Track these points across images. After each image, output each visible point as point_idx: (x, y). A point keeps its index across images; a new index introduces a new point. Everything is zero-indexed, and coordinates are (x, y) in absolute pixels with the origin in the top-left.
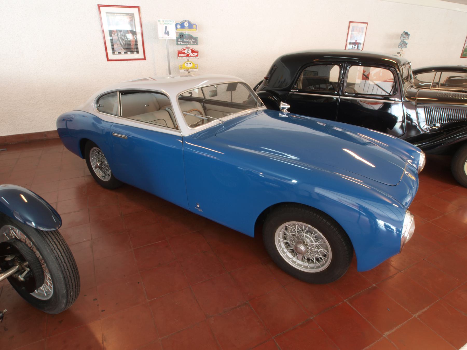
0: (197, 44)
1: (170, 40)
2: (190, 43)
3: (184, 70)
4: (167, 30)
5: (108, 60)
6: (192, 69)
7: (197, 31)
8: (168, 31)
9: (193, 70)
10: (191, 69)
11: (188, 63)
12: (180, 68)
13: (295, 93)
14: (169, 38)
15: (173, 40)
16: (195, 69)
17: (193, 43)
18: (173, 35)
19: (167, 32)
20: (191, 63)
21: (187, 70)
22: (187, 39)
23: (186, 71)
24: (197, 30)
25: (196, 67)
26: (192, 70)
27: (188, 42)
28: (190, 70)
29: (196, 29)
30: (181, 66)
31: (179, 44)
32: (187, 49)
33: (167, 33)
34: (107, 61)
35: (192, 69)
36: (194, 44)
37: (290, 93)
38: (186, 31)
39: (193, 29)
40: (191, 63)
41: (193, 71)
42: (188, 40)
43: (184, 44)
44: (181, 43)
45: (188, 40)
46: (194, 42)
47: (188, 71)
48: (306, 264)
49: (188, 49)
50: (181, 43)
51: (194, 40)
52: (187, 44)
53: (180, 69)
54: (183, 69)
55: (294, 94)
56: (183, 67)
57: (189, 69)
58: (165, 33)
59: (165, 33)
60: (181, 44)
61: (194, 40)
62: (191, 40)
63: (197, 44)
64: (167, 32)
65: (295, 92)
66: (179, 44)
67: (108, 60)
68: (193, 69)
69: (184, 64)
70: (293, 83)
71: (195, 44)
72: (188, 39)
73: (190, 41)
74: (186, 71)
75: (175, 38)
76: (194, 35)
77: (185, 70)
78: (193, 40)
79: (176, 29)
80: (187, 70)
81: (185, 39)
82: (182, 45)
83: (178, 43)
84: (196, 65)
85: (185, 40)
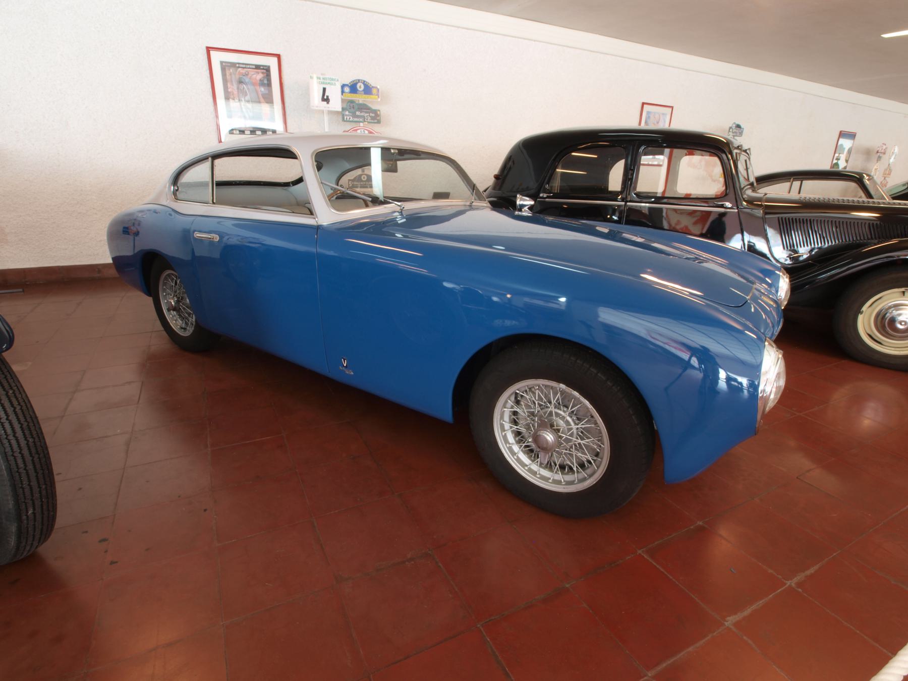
0: (379, 122)
1: (331, 113)
2: (367, 120)
4: (327, 94)
7: (379, 100)
8: (327, 97)
13: (547, 199)
14: (328, 108)
15: (337, 112)
17: (371, 120)
18: (336, 103)
19: (325, 97)
22: (361, 112)
24: (379, 97)
27: (364, 117)
29: (377, 97)
31: (347, 118)
32: (360, 130)
33: (325, 99)
36: (373, 121)
37: (538, 199)
38: (360, 98)
39: (372, 96)
42: (362, 114)
43: (356, 119)
44: (350, 118)
45: (362, 114)
46: (373, 118)
48: (559, 476)
49: (362, 130)
50: (350, 118)
51: (373, 115)
52: (361, 120)
55: (545, 201)
58: (323, 100)
59: (323, 100)
60: (351, 120)
61: (373, 115)
62: (368, 114)
63: (379, 122)
64: (325, 97)
65: (548, 197)
66: (347, 118)
70: (544, 182)
71: (376, 121)
72: (364, 112)
73: (367, 116)
75: (340, 110)
76: (374, 107)
78: (371, 114)
79: (342, 94)
81: (357, 113)
82: (351, 121)
83: (345, 117)
85: (357, 114)
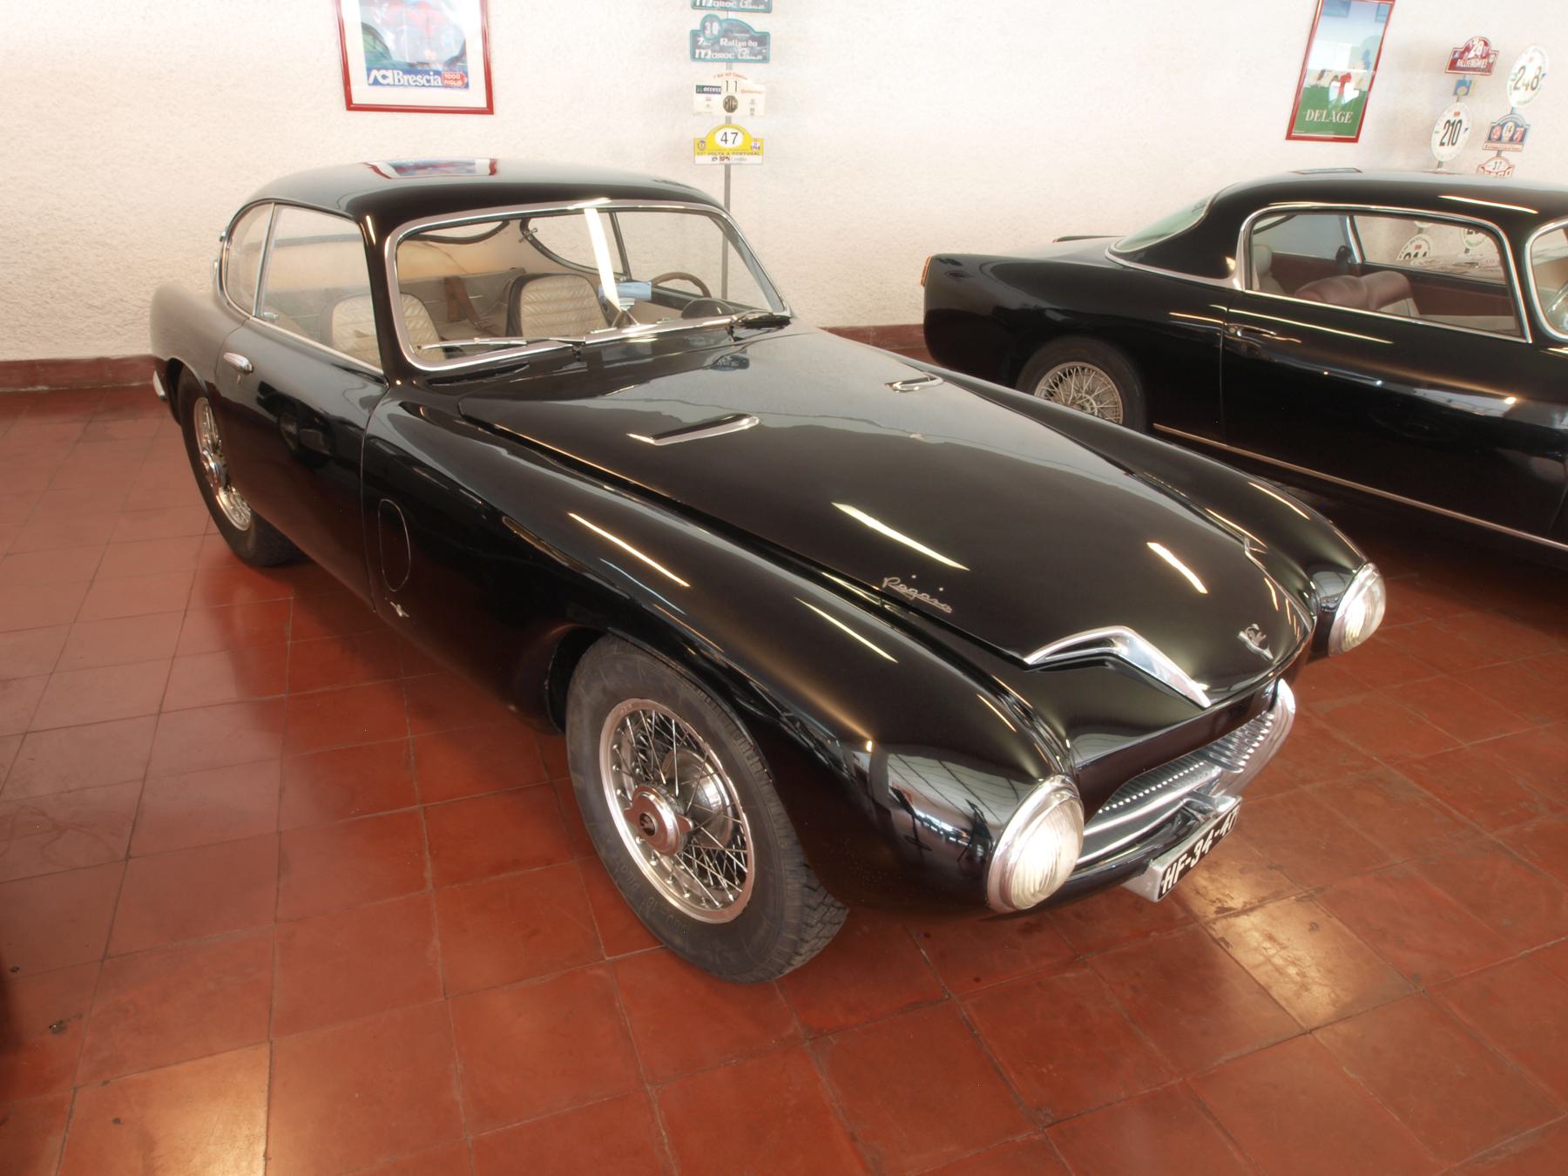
3: (711, 156)
5: (350, 106)
9: (744, 160)
10: (737, 154)
11: (729, 131)
12: (697, 150)
16: (752, 154)
20: (736, 131)
21: (722, 159)
23: (718, 161)
25: (756, 150)
26: (741, 159)
28: (734, 158)
30: (703, 142)
34: (345, 108)
35: (739, 157)
40: (740, 134)
41: (743, 162)
47: (726, 161)
53: (698, 154)
54: (709, 154)
57: (731, 156)
67: (350, 106)
68: (746, 156)
69: (715, 133)
74: (718, 161)
77: (713, 159)
80: (722, 159)
84: (756, 140)
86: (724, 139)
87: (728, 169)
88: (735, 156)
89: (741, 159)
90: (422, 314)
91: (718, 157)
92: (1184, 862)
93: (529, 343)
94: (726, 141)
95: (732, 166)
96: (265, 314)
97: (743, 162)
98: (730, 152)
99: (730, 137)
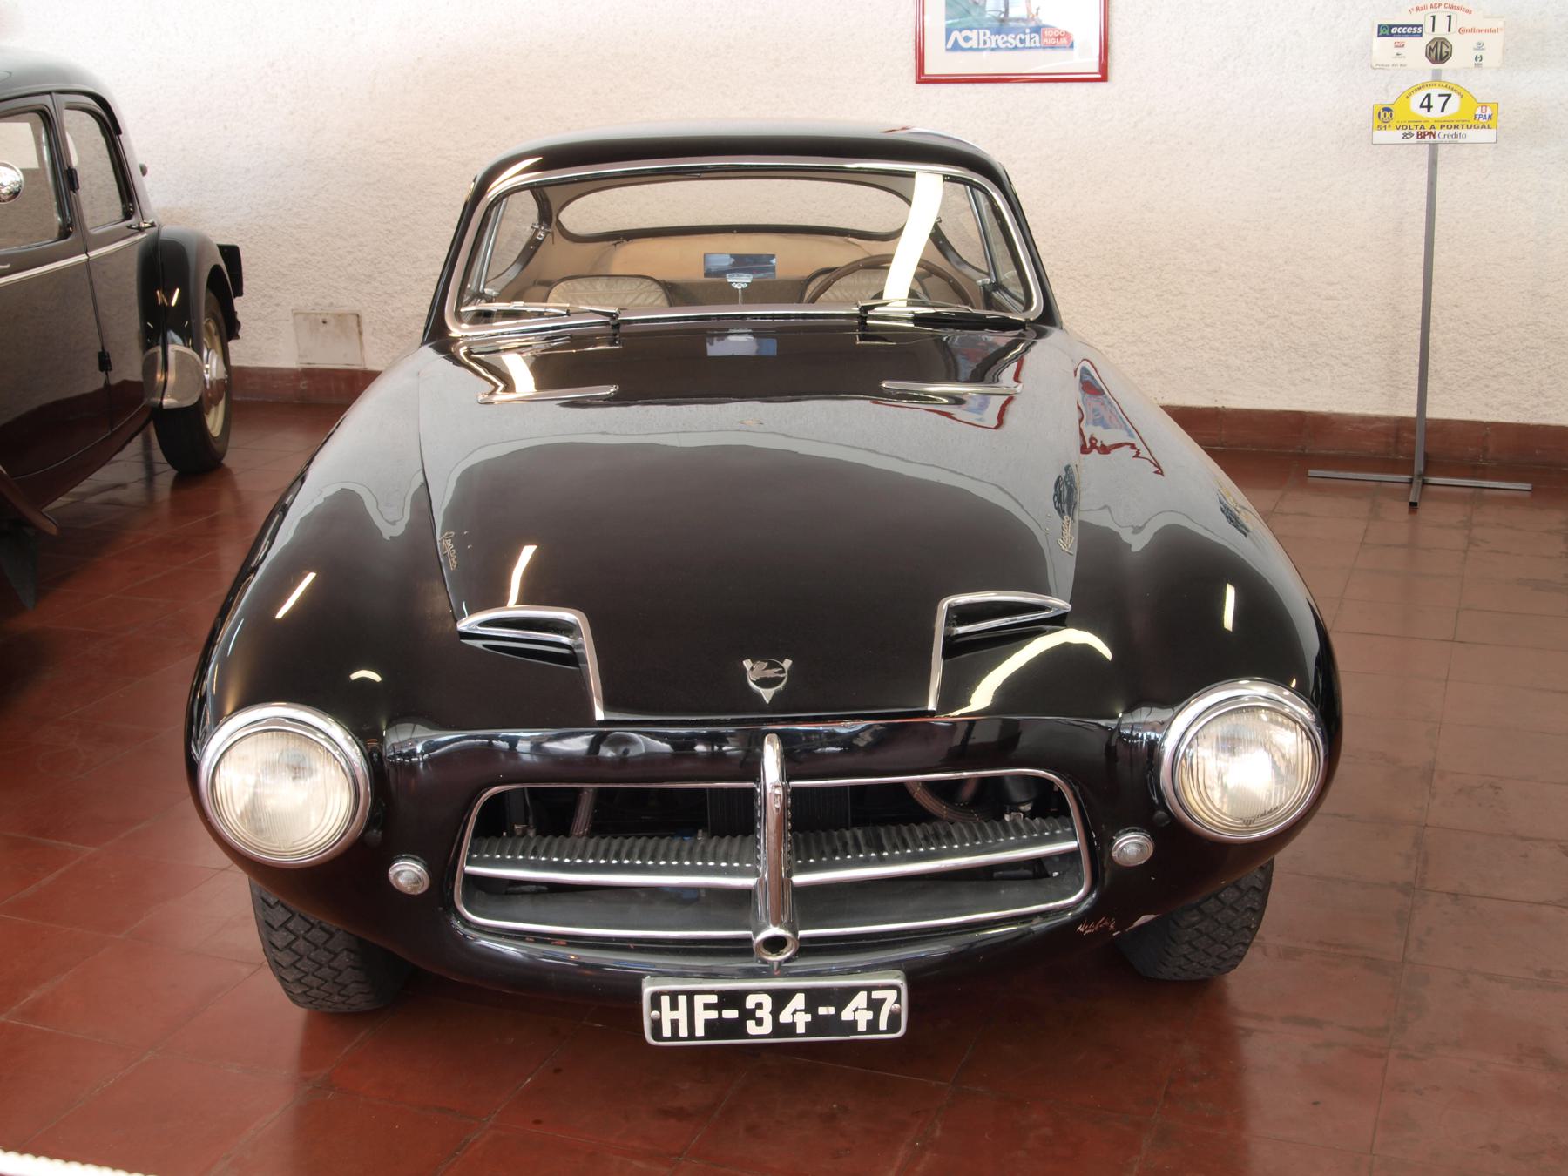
3: (1402, 132)
6: (1456, 127)
12: (1379, 123)
23: (1413, 139)
26: (1455, 135)
28: (1442, 133)
30: (1388, 110)
35: (1452, 131)
40: (1455, 98)
41: (1460, 140)
53: (1379, 128)
56: (1399, 116)
57: (1438, 131)
68: (1460, 131)
77: (1405, 136)
86: (1425, 103)
87: (1434, 148)
88: (1445, 131)
89: (1455, 135)
90: (659, 302)
91: (1415, 132)
92: (707, 1007)
93: (568, 314)
94: (1429, 107)
95: (1442, 150)
96: (486, 290)
97: (1460, 140)
98: (1437, 125)
99: (1437, 102)
